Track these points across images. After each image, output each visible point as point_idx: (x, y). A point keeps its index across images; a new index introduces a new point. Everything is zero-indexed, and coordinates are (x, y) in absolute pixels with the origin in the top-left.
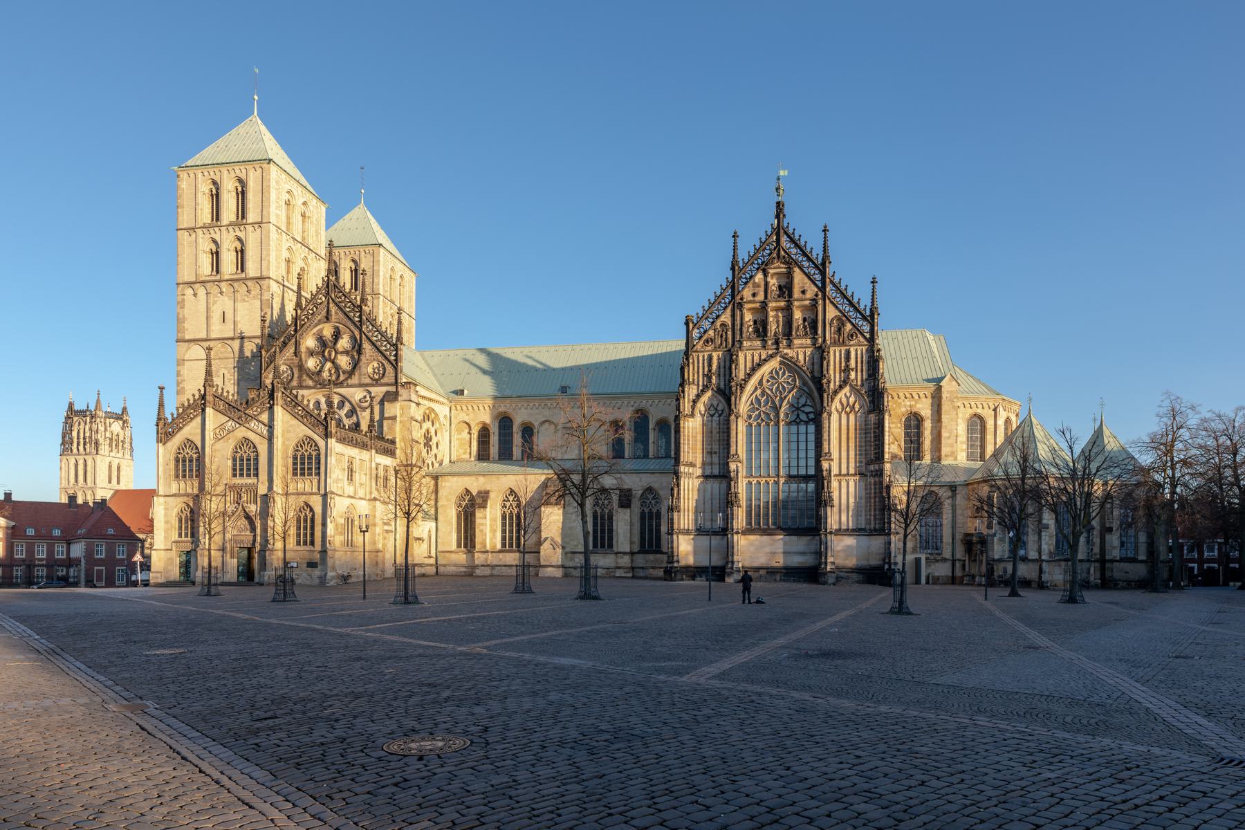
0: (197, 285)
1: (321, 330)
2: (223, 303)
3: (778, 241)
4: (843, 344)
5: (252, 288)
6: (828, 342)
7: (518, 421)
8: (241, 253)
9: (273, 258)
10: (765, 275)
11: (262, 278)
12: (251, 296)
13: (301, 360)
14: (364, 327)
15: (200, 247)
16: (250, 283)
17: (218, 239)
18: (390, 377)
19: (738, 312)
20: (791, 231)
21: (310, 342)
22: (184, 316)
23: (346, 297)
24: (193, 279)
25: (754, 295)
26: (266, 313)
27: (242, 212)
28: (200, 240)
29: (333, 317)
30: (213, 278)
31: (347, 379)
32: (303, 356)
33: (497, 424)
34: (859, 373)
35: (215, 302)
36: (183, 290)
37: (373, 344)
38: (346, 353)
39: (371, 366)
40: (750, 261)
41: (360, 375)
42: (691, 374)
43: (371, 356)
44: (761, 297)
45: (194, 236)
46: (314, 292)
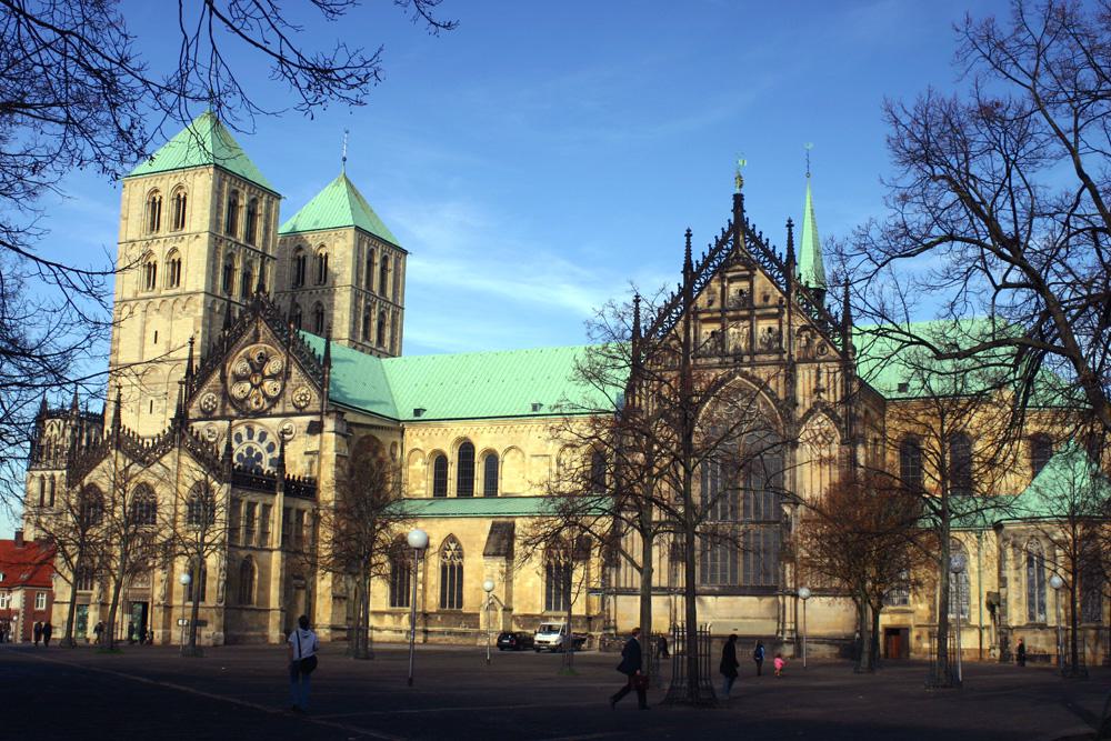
0: (133, 303)
1: (247, 353)
2: (158, 322)
3: (736, 239)
4: (813, 360)
6: (795, 358)
7: (479, 448)
8: (176, 266)
10: (722, 279)
13: (226, 386)
16: (184, 299)
18: (315, 406)
19: (692, 323)
20: (751, 227)
21: (237, 366)
25: (711, 303)
27: (180, 221)
31: (270, 408)
32: (229, 383)
33: (457, 452)
34: (832, 395)
37: (301, 367)
38: (273, 377)
40: (707, 260)
41: (284, 402)
42: (637, 398)
43: (296, 381)
44: (717, 305)
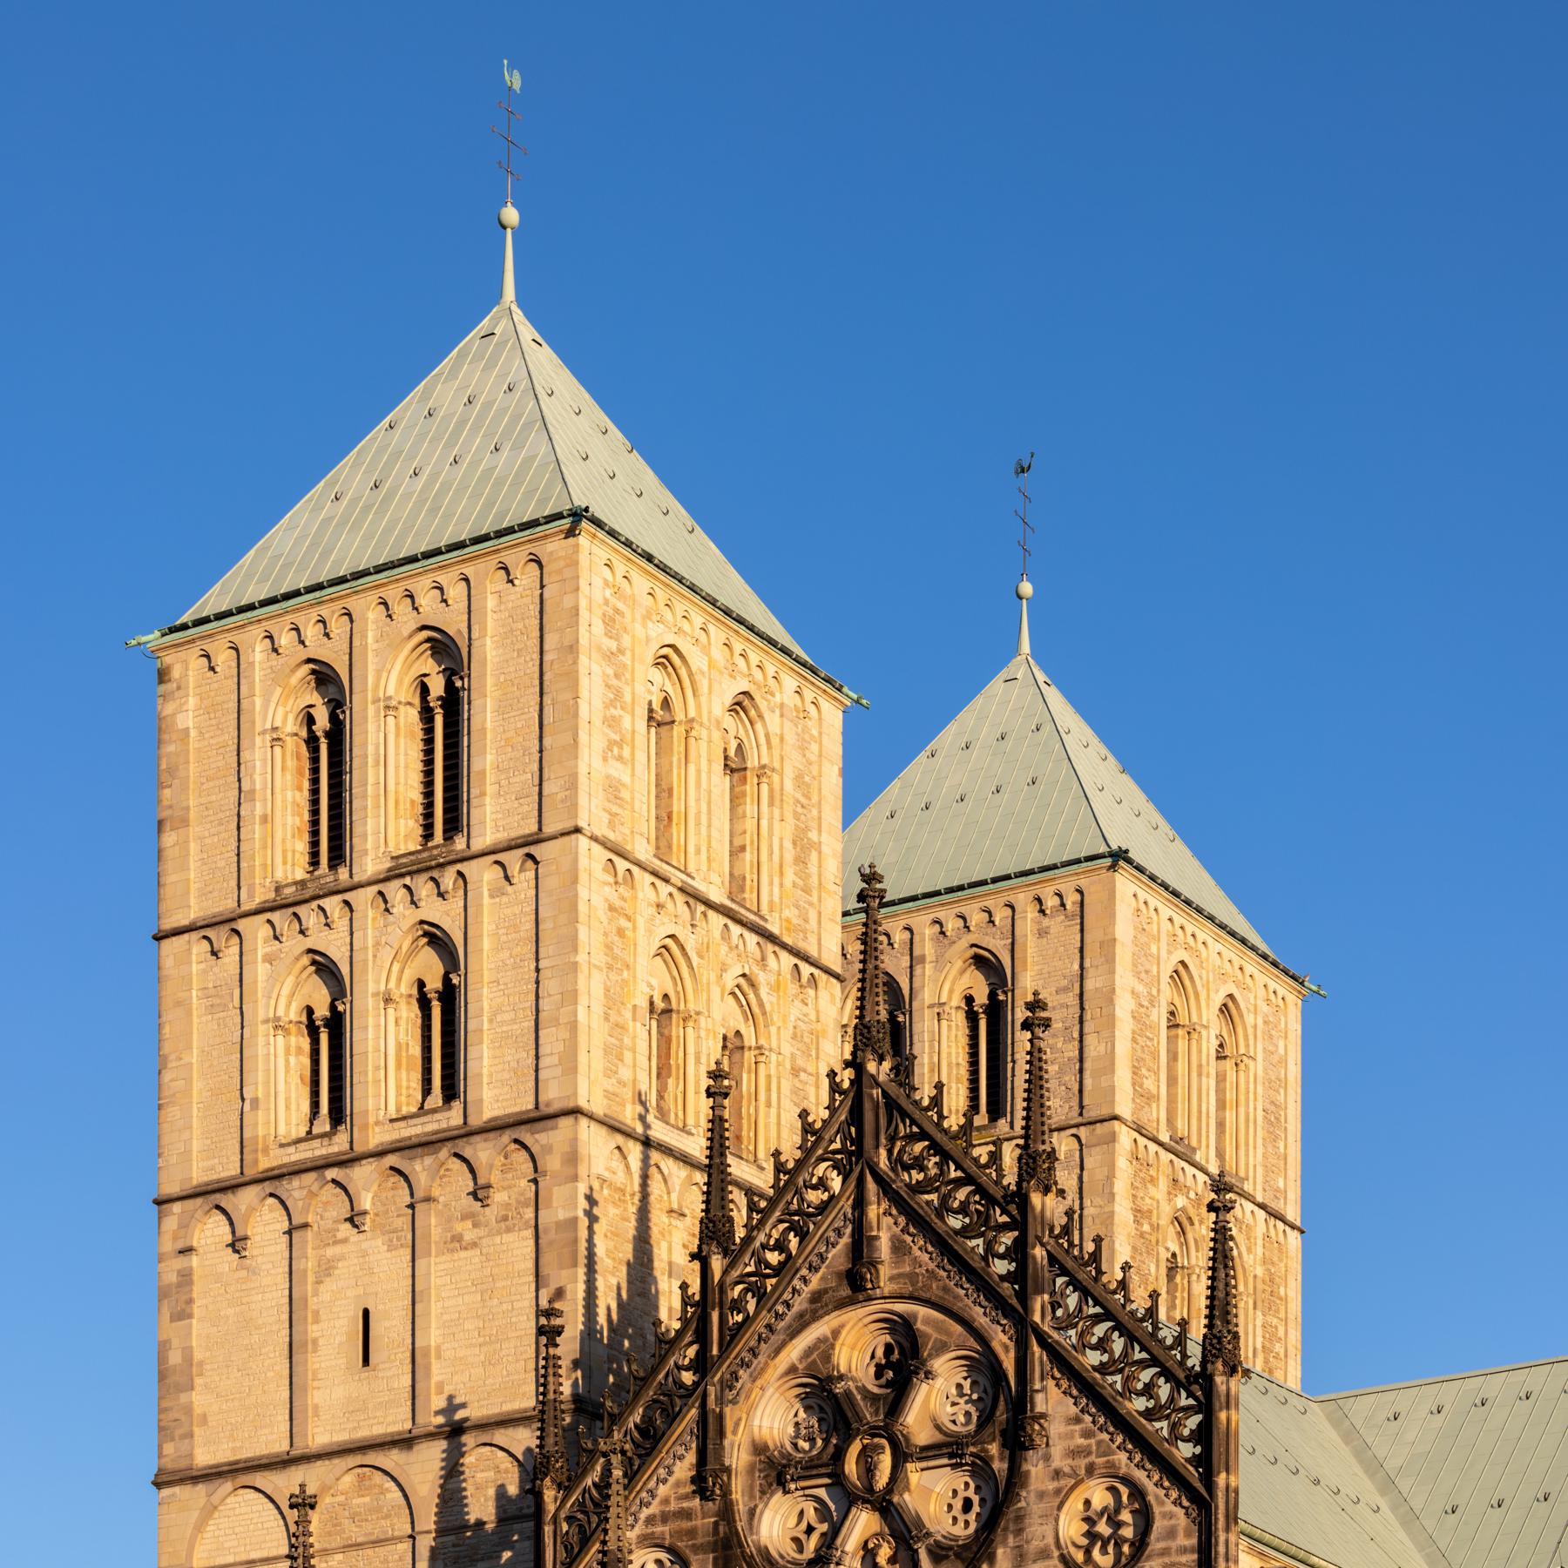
0: (249, 1195)
1: (825, 1347)
5: (495, 1178)
9: (590, 1013)
11: (539, 1118)
12: (491, 1213)
13: (727, 1513)
14: (1039, 1302)
15: (260, 1010)
16: (483, 1152)
17: (339, 954)
22: (188, 1353)
23: (946, 1157)
24: (230, 1170)
26: (559, 1294)
28: (260, 972)
29: (885, 1271)
30: (318, 1150)
35: (326, 1269)
36: (184, 1226)
39: (1075, 1505)
45: (231, 954)
46: (790, 1155)
